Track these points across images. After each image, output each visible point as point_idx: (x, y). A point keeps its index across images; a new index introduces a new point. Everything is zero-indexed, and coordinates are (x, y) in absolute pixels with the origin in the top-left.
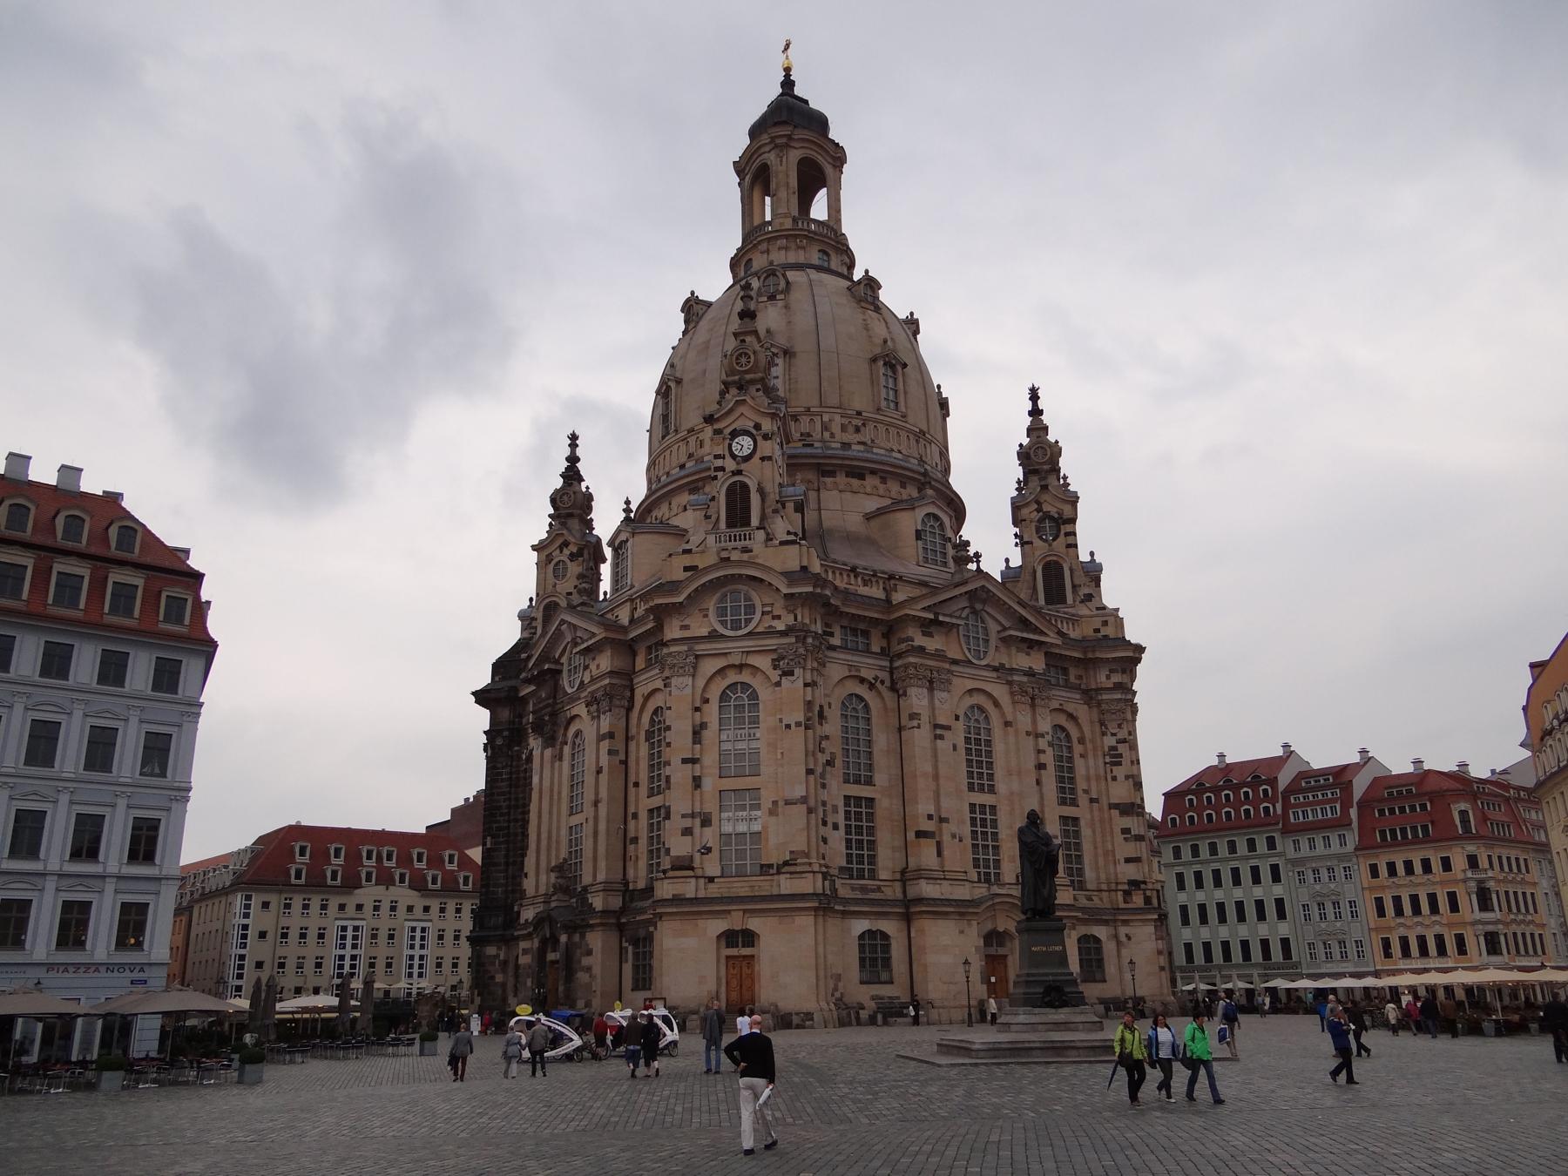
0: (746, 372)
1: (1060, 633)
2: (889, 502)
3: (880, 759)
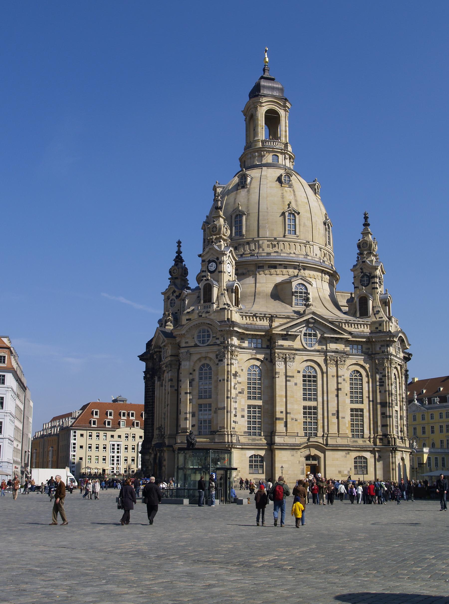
0: (214, 235)
1: (350, 333)
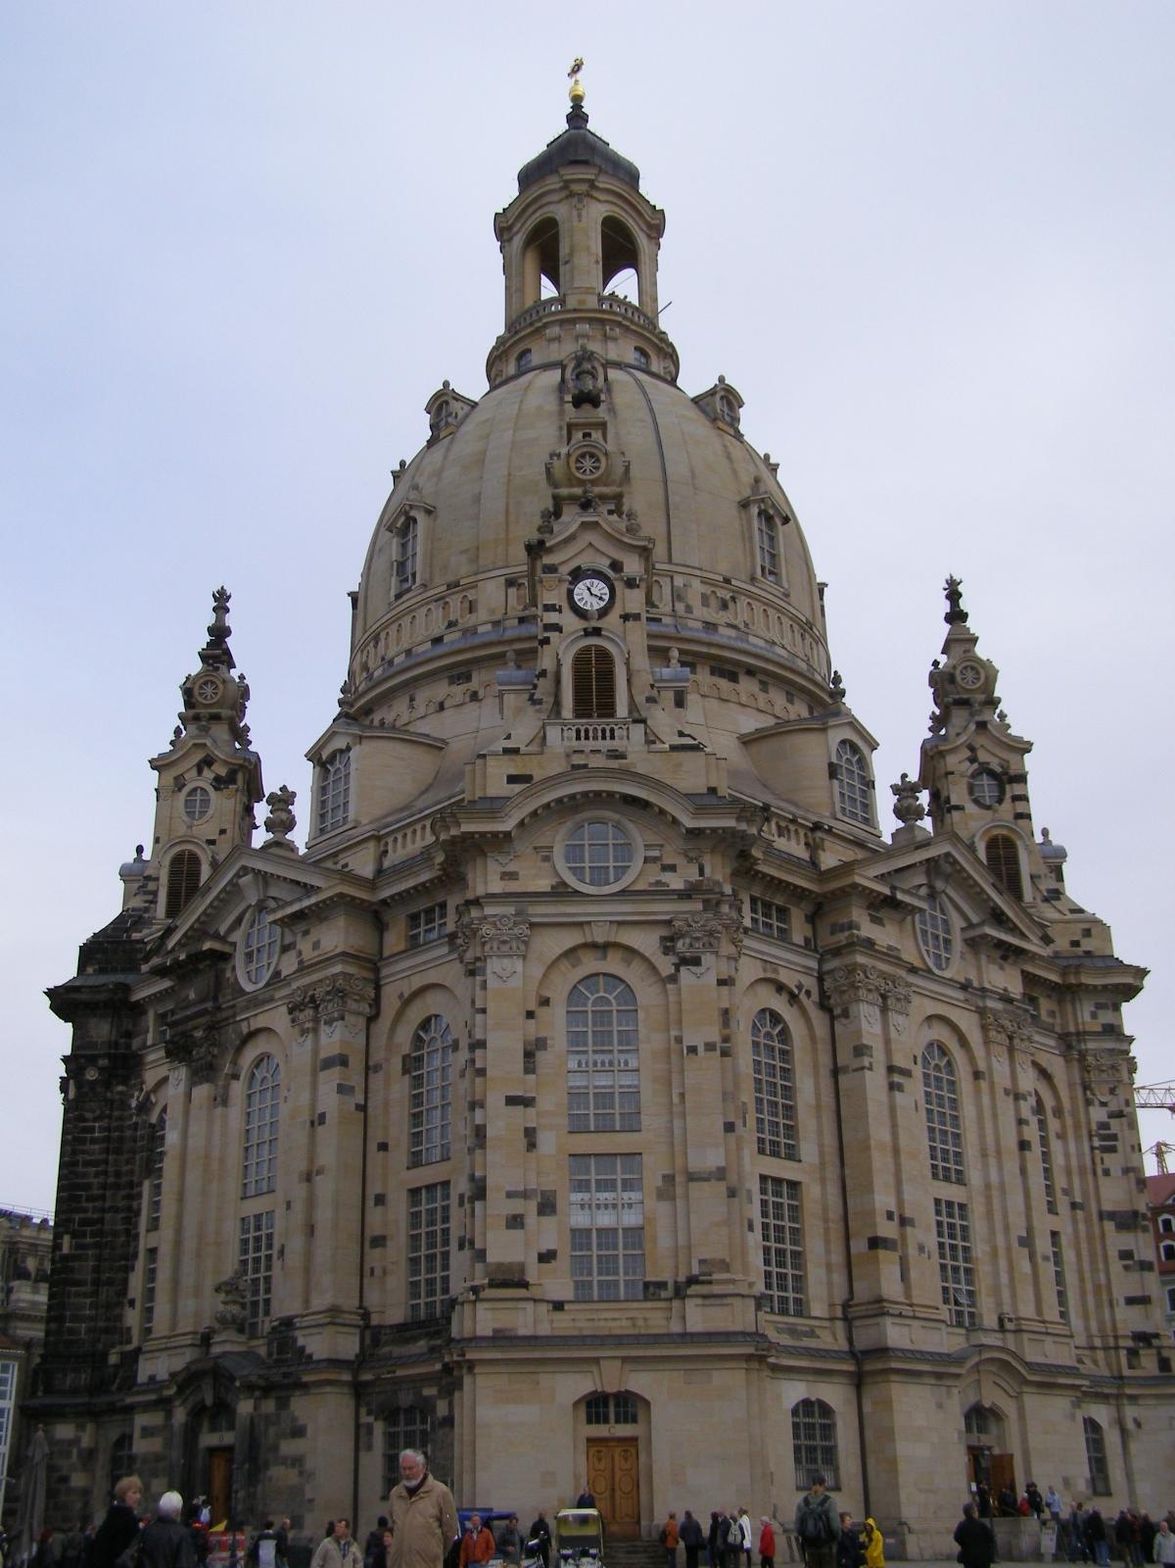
1: (1047, 940)
2: (771, 722)
3: (806, 1121)
